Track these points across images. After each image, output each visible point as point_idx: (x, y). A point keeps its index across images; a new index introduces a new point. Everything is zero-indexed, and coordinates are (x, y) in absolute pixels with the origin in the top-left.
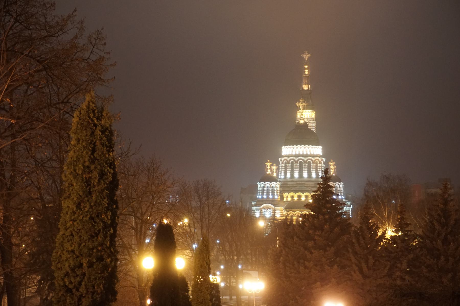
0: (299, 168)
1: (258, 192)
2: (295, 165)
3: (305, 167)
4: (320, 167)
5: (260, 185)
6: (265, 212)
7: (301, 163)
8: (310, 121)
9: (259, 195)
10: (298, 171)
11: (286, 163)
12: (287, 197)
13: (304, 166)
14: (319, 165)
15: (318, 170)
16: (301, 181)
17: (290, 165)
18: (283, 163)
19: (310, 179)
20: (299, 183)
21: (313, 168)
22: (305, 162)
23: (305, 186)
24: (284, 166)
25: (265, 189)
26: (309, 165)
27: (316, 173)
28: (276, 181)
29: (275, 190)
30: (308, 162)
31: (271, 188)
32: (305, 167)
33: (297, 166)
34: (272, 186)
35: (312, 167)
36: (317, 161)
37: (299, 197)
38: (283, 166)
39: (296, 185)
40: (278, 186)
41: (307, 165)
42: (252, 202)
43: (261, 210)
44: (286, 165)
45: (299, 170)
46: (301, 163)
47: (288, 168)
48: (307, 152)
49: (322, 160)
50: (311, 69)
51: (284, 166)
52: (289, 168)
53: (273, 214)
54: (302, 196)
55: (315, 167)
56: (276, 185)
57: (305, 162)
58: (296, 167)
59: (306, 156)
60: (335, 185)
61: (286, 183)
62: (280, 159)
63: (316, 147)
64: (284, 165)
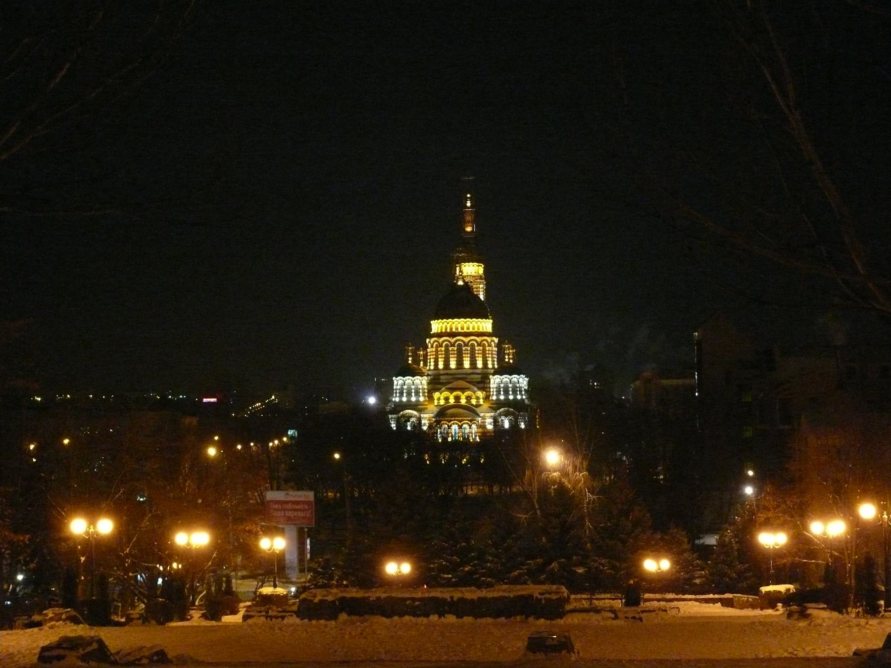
0: (457, 354)
1: (394, 391)
2: (450, 349)
4: (490, 352)
5: (398, 382)
7: (459, 346)
8: (477, 279)
9: (396, 396)
11: (437, 347)
12: (439, 399)
13: (465, 350)
14: (487, 348)
15: (486, 357)
16: (461, 374)
18: (432, 347)
19: (474, 371)
20: (457, 376)
21: (478, 353)
22: (466, 345)
23: (467, 382)
25: (405, 387)
26: (472, 349)
27: (483, 361)
28: (421, 374)
29: (419, 389)
32: (466, 352)
34: (415, 382)
35: (477, 352)
36: (485, 342)
37: (457, 398)
38: (433, 352)
39: (452, 381)
41: (469, 348)
45: (457, 357)
46: (460, 346)
47: (440, 354)
49: (493, 341)
52: (442, 354)
54: (461, 397)
56: (421, 382)
58: (453, 352)
59: (467, 335)
61: (437, 377)
62: (428, 340)
63: (483, 321)
64: (434, 350)
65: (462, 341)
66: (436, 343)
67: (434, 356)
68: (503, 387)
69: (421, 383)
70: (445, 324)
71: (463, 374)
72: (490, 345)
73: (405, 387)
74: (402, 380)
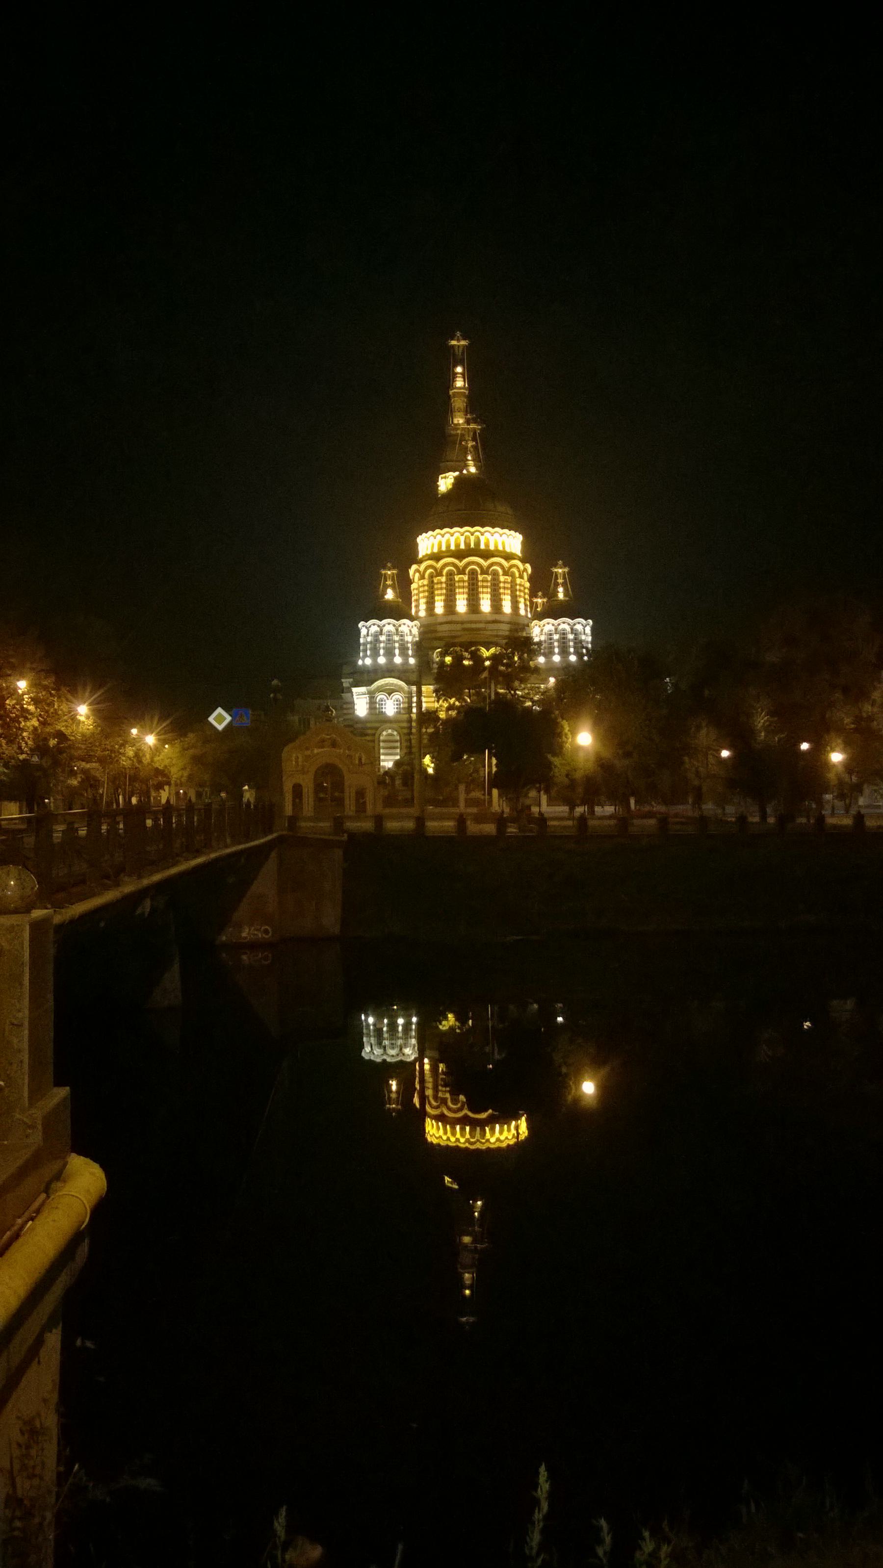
1: (361, 648)
2: (457, 578)
3: (485, 584)
5: (368, 629)
6: (383, 703)
7: (473, 573)
9: (365, 656)
10: (466, 596)
11: (431, 576)
13: (483, 581)
14: (518, 581)
15: (516, 596)
16: (476, 622)
17: (444, 579)
18: (422, 577)
21: (504, 588)
22: (484, 572)
24: (427, 585)
25: (383, 638)
26: (493, 579)
29: (407, 642)
30: (493, 570)
31: (397, 634)
32: (485, 584)
33: (464, 581)
34: (400, 629)
35: (502, 585)
36: (514, 570)
40: (415, 631)
41: (489, 578)
42: (343, 680)
43: (372, 695)
44: (433, 582)
45: (469, 594)
46: (473, 573)
47: (438, 589)
48: (487, 545)
50: (470, 377)
51: (427, 585)
52: (441, 589)
53: (406, 705)
55: (509, 586)
57: (484, 572)
58: (461, 584)
60: (575, 625)
64: (426, 582)
65: (478, 564)
66: (430, 570)
67: (426, 594)
68: (558, 641)
69: (410, 631)
70: (447, 536)
71: (480, 622)
72: (521, 577)
73: (383, 638)
74: (376, 626)
